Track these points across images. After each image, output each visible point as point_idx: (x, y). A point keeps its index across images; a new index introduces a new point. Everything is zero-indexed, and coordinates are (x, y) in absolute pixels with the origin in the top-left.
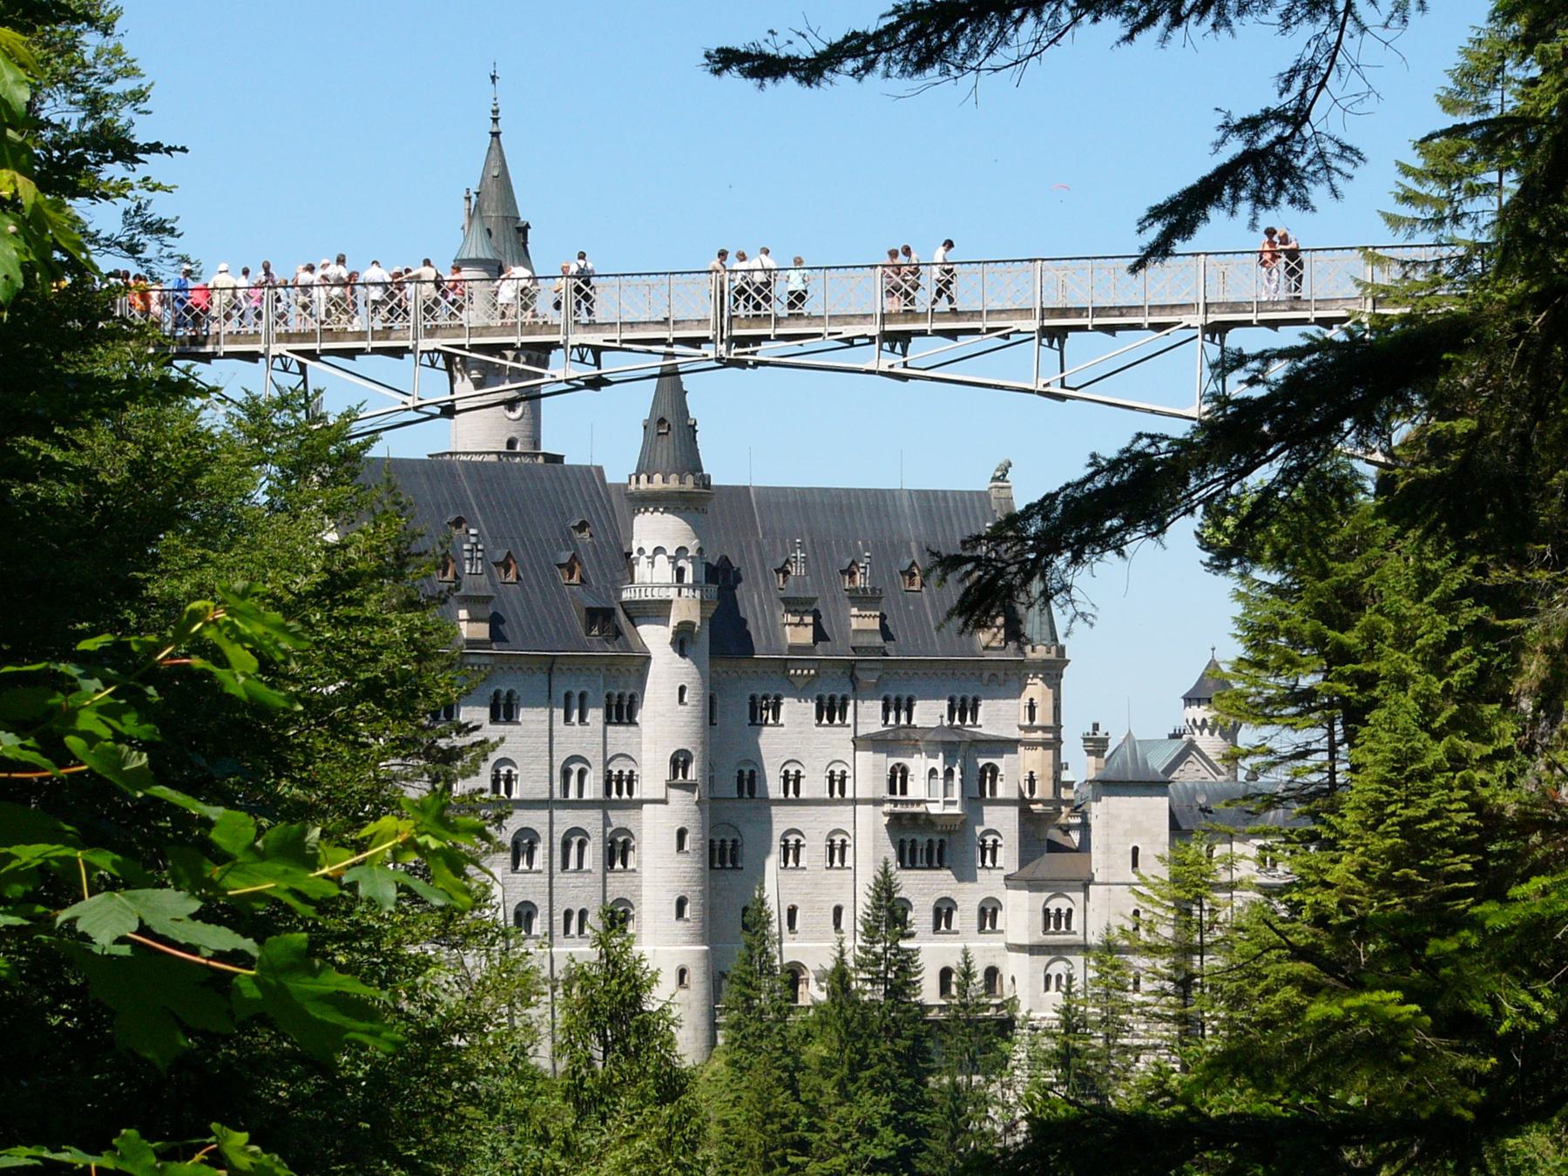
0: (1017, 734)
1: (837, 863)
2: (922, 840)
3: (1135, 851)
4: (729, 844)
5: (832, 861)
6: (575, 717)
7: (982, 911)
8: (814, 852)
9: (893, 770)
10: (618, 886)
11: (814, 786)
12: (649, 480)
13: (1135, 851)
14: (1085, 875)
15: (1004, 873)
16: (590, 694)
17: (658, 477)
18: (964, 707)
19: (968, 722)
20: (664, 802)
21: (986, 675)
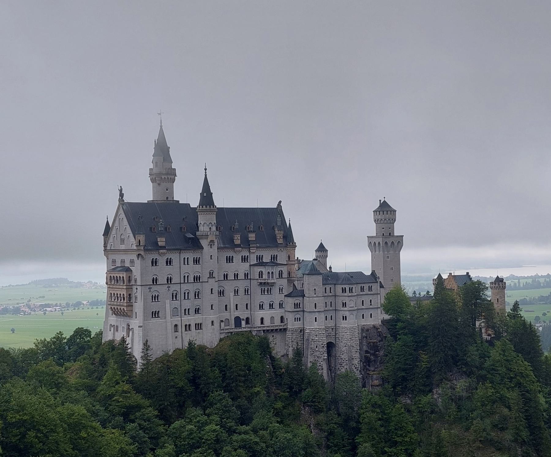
0: (286, 264)
1: (246, 294)
2: (266, 289)
3: (315, 289)
4: (222, 291)
5: (245, 293)
6: (186, 263)
7: (280, 303)
8: (241, 292)
9: (259, 272)
10: (197, 302)
11: (241, 276)
12: (202, 207)
13: (315, 289)
14: (302, 295)
15: (284, 295)
16: (189, 257)
17: (204, 206)
18: (274, 258)
19: (275, 260)
20: (207, 282)
21: (279, 250)
